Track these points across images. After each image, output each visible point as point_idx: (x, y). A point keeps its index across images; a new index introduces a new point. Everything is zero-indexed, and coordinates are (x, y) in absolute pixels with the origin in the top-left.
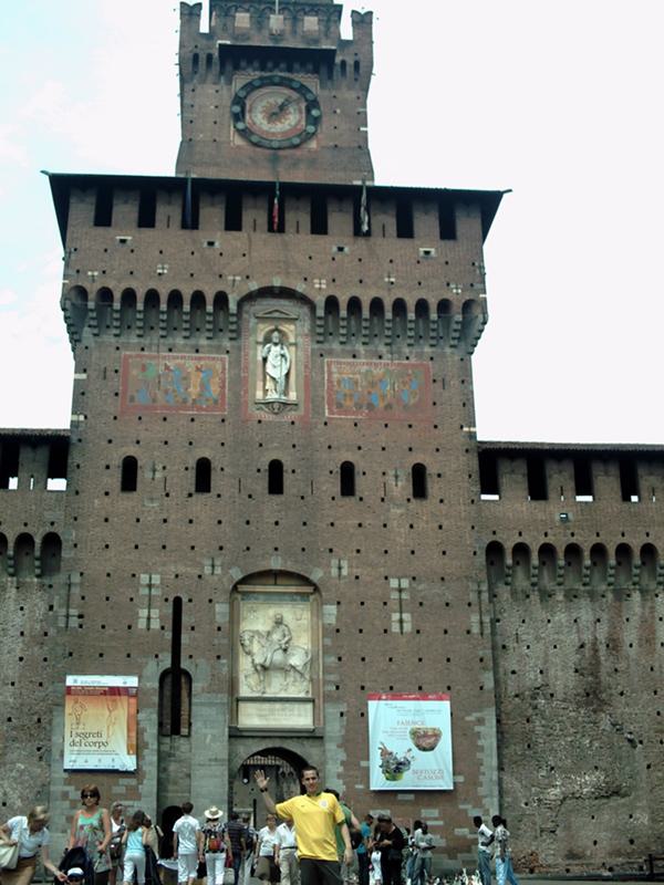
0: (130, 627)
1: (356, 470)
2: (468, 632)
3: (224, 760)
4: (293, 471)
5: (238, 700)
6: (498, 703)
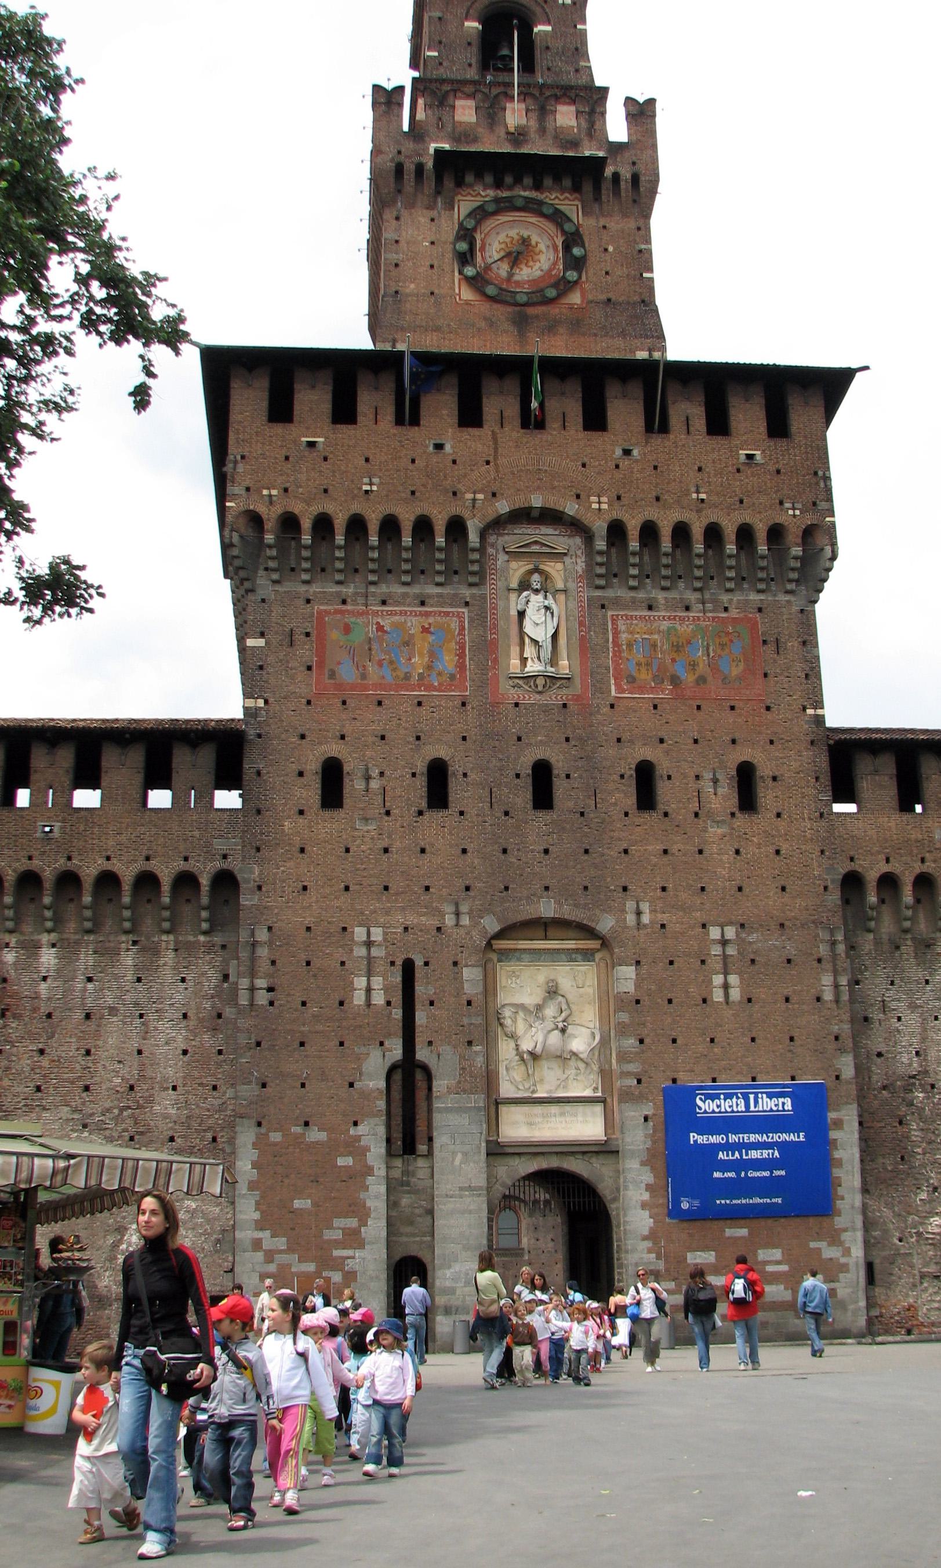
0: (341, 1003)
2: (818, 999)
3: (480, 1188)
4: (568, 776)
5: (497, 1104)
6: (861, 1098)
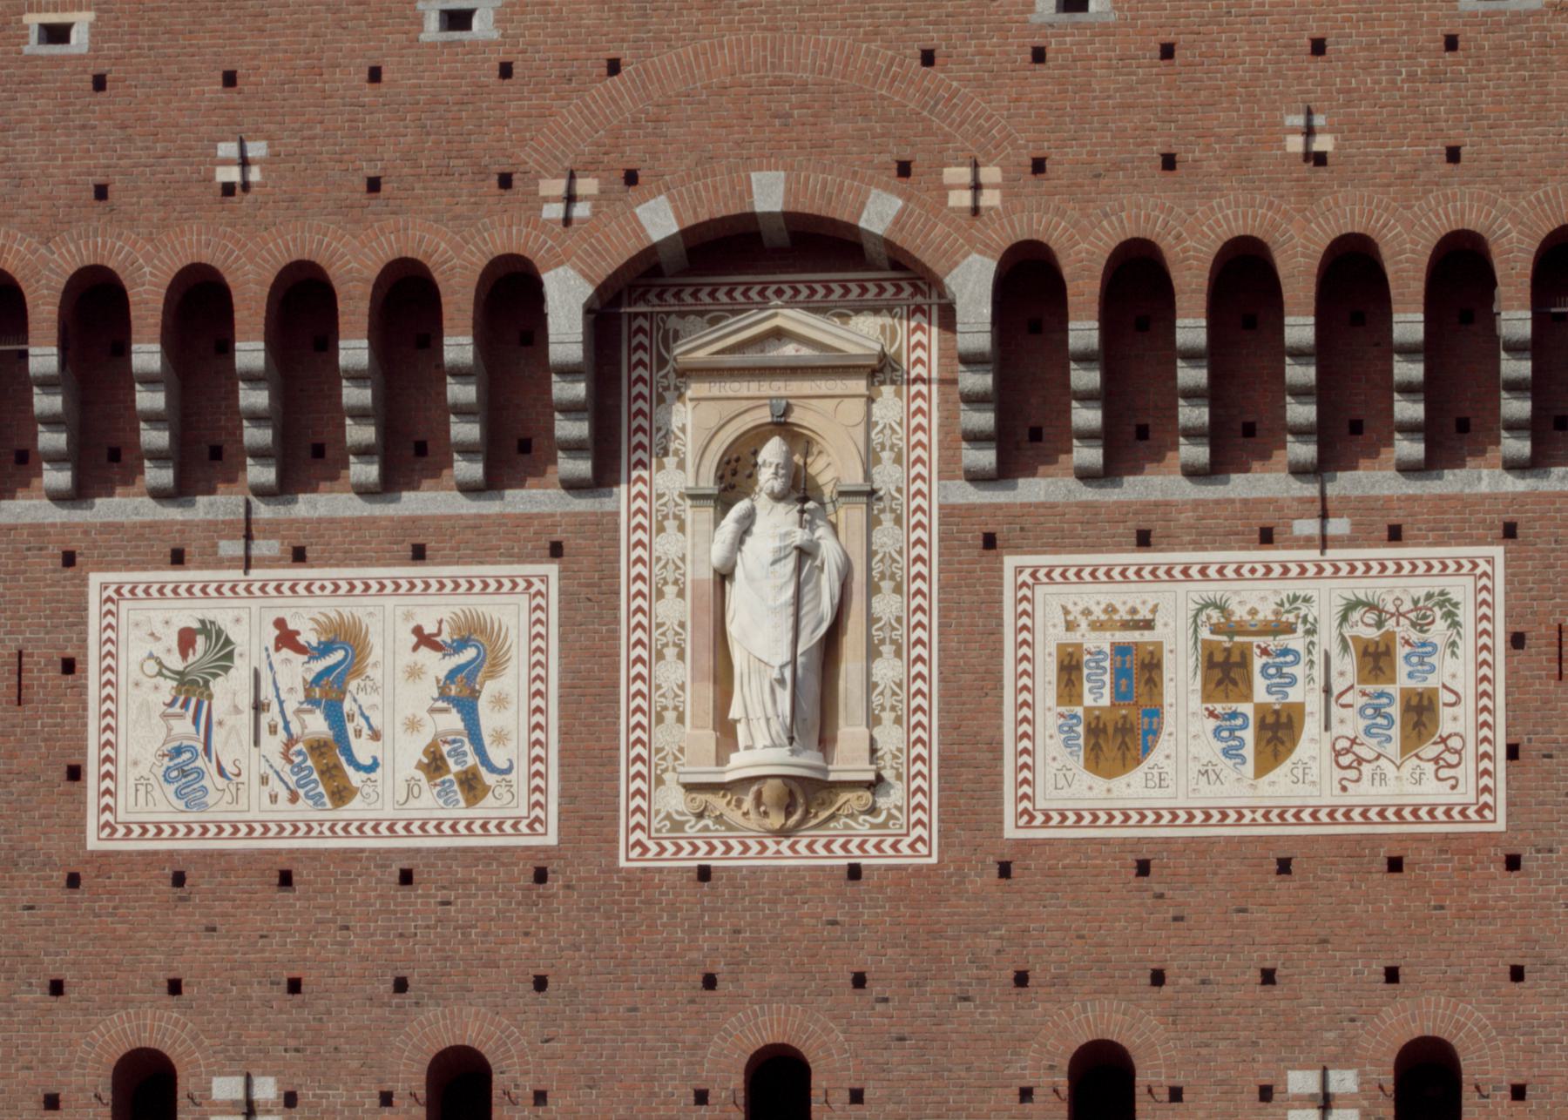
1: (1143, 1078)
